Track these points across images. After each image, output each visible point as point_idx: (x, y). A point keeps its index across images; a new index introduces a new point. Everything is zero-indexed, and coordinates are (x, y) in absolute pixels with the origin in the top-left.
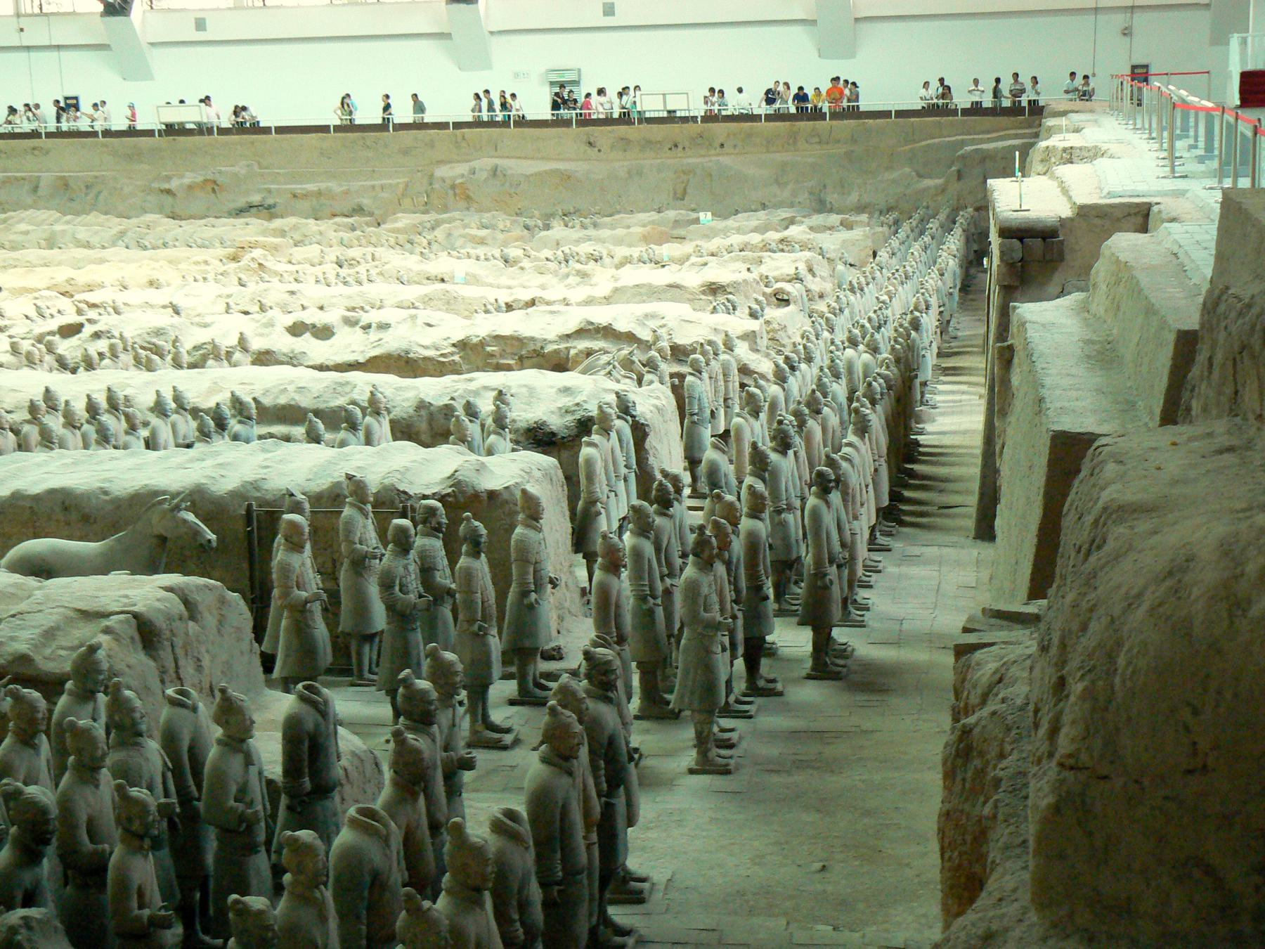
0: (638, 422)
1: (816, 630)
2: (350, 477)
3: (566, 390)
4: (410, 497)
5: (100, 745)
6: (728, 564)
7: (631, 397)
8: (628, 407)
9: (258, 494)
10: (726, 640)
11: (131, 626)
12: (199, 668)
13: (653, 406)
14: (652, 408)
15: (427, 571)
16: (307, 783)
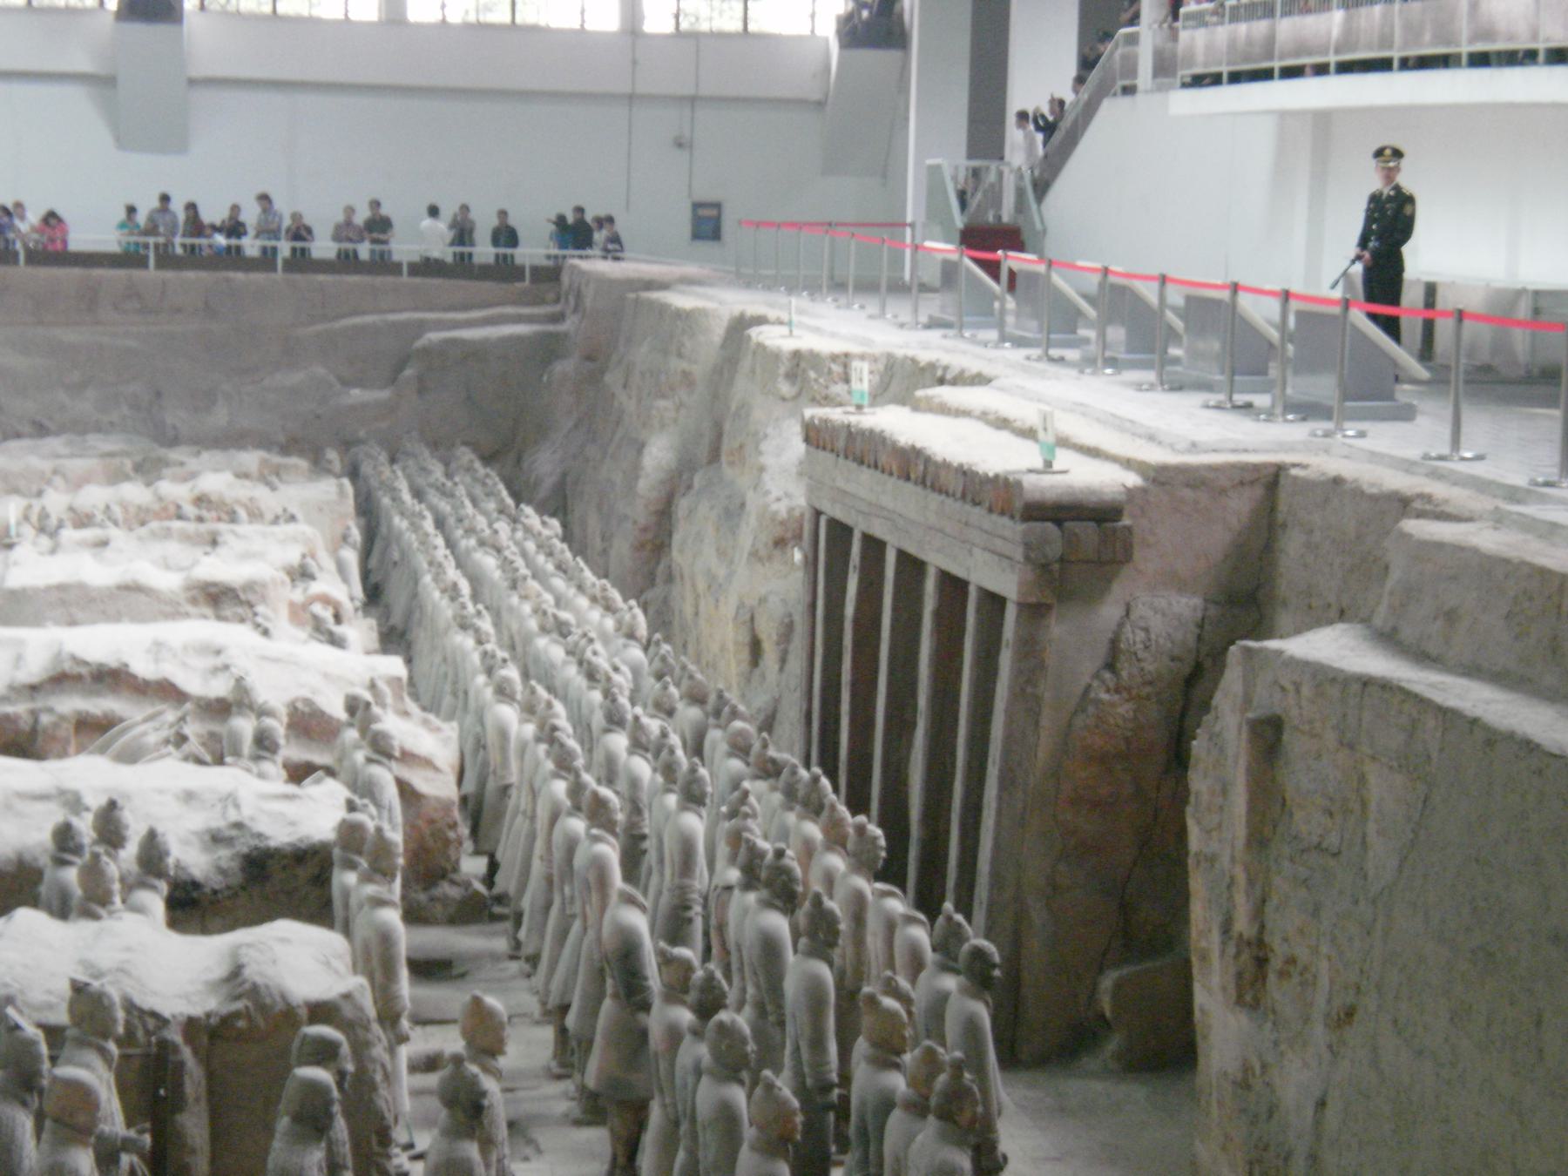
3: (189, 797)
4: (162, 1021)
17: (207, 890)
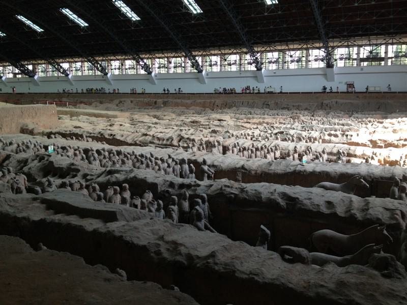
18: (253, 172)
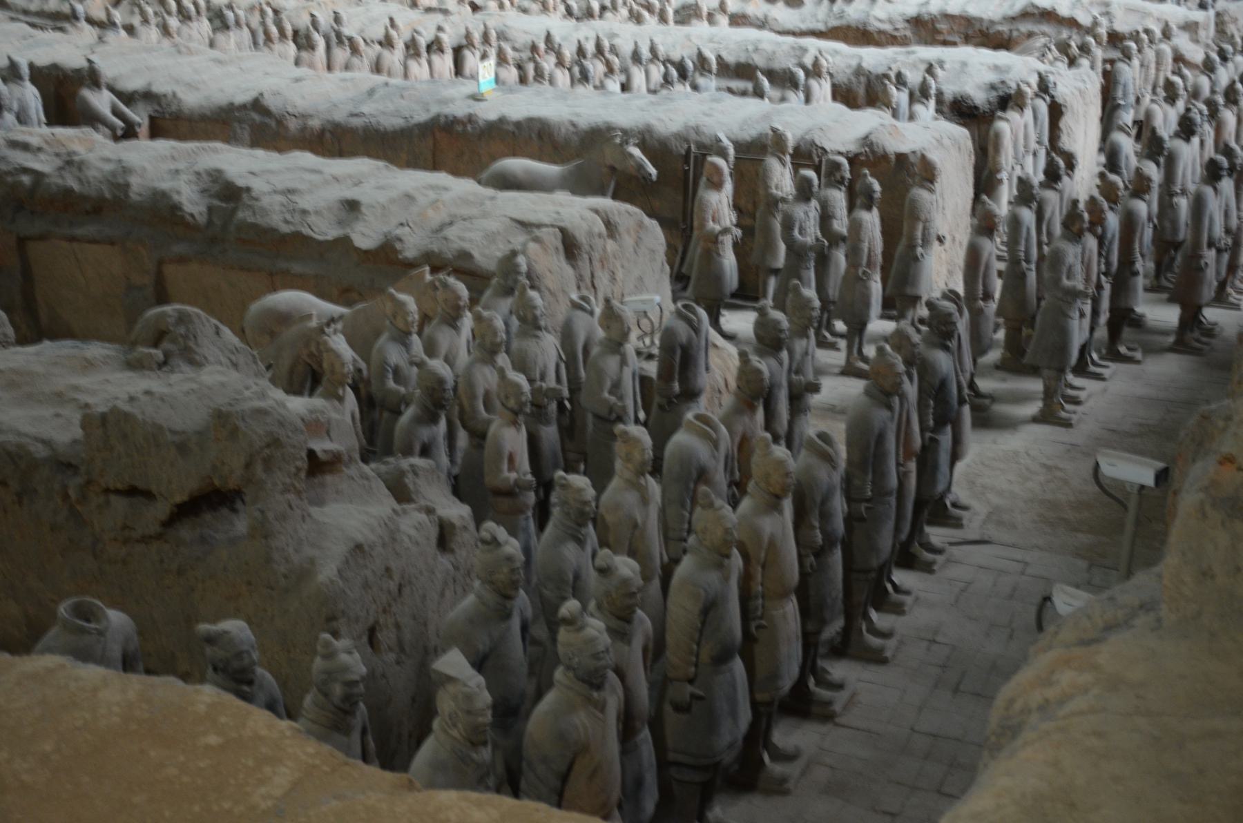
0: (1056, 102)
1: (1184, 307)
2: (774, 130)
3: (996, 68)
5: (499, 334)
6: (1101, 240)
7: (1051, 78)
8: (1047, 87)
9: (698, 138)
10: (1088, 309)
11: (556, 238)
12: (613, 279)
13: (1075, 88)
14: (1074, 91)
15: (826, 218)
16: (676, 386)
17: (981, 111)
18: (293, 125)
